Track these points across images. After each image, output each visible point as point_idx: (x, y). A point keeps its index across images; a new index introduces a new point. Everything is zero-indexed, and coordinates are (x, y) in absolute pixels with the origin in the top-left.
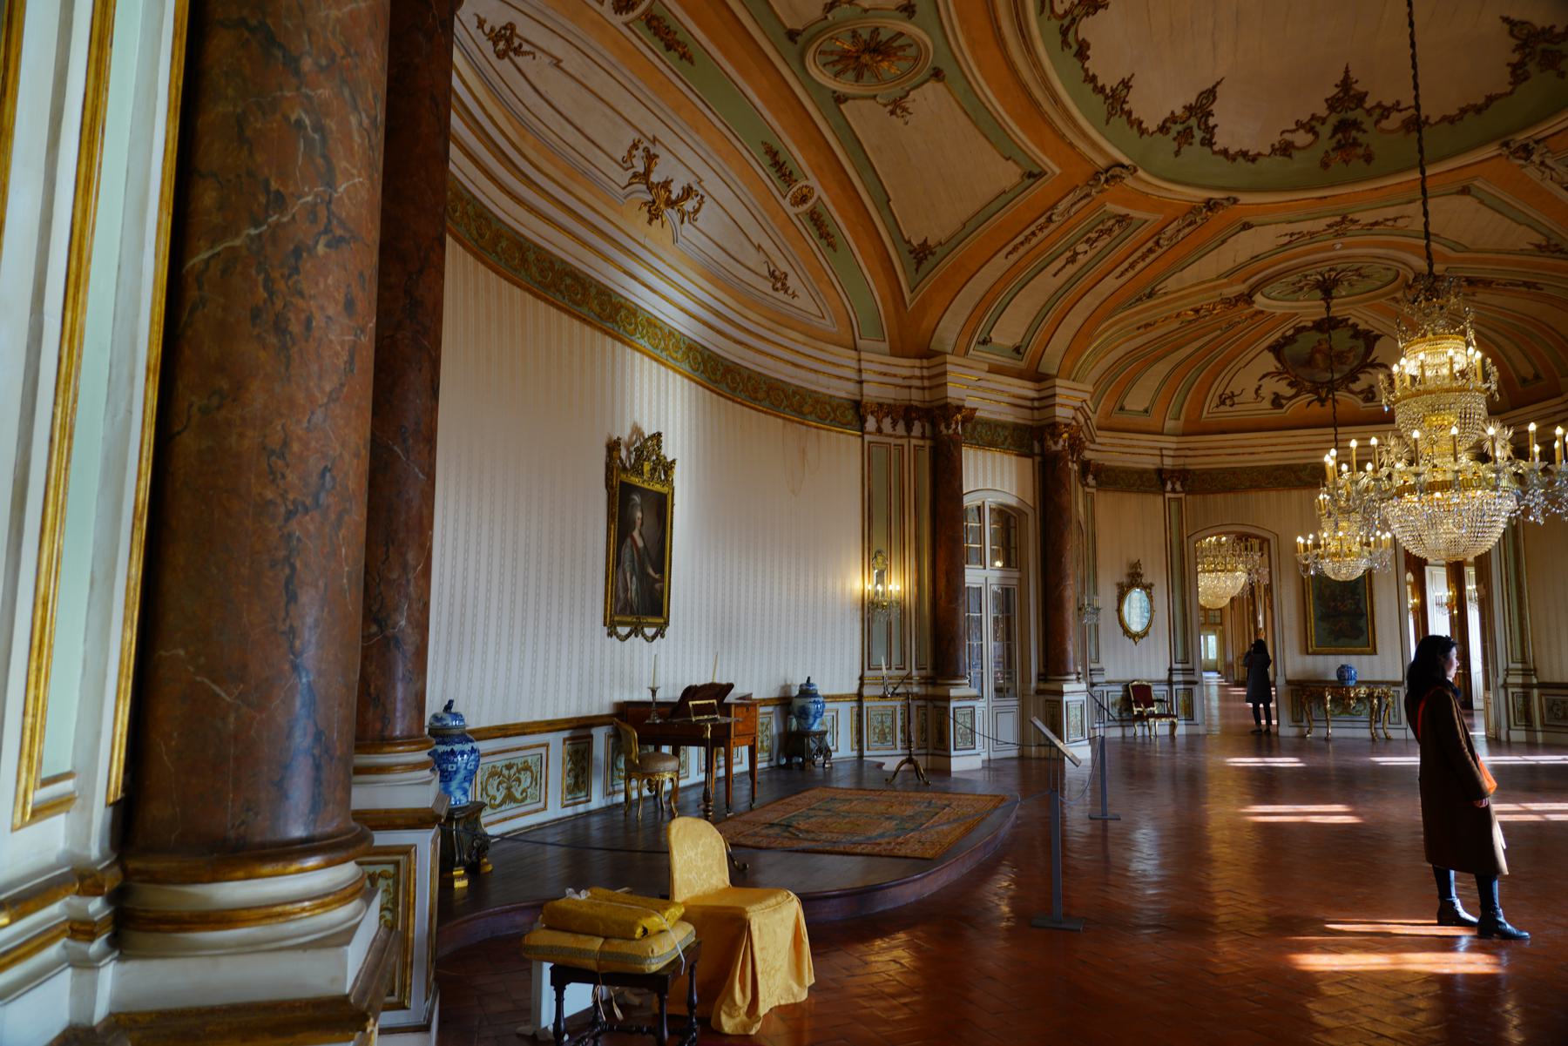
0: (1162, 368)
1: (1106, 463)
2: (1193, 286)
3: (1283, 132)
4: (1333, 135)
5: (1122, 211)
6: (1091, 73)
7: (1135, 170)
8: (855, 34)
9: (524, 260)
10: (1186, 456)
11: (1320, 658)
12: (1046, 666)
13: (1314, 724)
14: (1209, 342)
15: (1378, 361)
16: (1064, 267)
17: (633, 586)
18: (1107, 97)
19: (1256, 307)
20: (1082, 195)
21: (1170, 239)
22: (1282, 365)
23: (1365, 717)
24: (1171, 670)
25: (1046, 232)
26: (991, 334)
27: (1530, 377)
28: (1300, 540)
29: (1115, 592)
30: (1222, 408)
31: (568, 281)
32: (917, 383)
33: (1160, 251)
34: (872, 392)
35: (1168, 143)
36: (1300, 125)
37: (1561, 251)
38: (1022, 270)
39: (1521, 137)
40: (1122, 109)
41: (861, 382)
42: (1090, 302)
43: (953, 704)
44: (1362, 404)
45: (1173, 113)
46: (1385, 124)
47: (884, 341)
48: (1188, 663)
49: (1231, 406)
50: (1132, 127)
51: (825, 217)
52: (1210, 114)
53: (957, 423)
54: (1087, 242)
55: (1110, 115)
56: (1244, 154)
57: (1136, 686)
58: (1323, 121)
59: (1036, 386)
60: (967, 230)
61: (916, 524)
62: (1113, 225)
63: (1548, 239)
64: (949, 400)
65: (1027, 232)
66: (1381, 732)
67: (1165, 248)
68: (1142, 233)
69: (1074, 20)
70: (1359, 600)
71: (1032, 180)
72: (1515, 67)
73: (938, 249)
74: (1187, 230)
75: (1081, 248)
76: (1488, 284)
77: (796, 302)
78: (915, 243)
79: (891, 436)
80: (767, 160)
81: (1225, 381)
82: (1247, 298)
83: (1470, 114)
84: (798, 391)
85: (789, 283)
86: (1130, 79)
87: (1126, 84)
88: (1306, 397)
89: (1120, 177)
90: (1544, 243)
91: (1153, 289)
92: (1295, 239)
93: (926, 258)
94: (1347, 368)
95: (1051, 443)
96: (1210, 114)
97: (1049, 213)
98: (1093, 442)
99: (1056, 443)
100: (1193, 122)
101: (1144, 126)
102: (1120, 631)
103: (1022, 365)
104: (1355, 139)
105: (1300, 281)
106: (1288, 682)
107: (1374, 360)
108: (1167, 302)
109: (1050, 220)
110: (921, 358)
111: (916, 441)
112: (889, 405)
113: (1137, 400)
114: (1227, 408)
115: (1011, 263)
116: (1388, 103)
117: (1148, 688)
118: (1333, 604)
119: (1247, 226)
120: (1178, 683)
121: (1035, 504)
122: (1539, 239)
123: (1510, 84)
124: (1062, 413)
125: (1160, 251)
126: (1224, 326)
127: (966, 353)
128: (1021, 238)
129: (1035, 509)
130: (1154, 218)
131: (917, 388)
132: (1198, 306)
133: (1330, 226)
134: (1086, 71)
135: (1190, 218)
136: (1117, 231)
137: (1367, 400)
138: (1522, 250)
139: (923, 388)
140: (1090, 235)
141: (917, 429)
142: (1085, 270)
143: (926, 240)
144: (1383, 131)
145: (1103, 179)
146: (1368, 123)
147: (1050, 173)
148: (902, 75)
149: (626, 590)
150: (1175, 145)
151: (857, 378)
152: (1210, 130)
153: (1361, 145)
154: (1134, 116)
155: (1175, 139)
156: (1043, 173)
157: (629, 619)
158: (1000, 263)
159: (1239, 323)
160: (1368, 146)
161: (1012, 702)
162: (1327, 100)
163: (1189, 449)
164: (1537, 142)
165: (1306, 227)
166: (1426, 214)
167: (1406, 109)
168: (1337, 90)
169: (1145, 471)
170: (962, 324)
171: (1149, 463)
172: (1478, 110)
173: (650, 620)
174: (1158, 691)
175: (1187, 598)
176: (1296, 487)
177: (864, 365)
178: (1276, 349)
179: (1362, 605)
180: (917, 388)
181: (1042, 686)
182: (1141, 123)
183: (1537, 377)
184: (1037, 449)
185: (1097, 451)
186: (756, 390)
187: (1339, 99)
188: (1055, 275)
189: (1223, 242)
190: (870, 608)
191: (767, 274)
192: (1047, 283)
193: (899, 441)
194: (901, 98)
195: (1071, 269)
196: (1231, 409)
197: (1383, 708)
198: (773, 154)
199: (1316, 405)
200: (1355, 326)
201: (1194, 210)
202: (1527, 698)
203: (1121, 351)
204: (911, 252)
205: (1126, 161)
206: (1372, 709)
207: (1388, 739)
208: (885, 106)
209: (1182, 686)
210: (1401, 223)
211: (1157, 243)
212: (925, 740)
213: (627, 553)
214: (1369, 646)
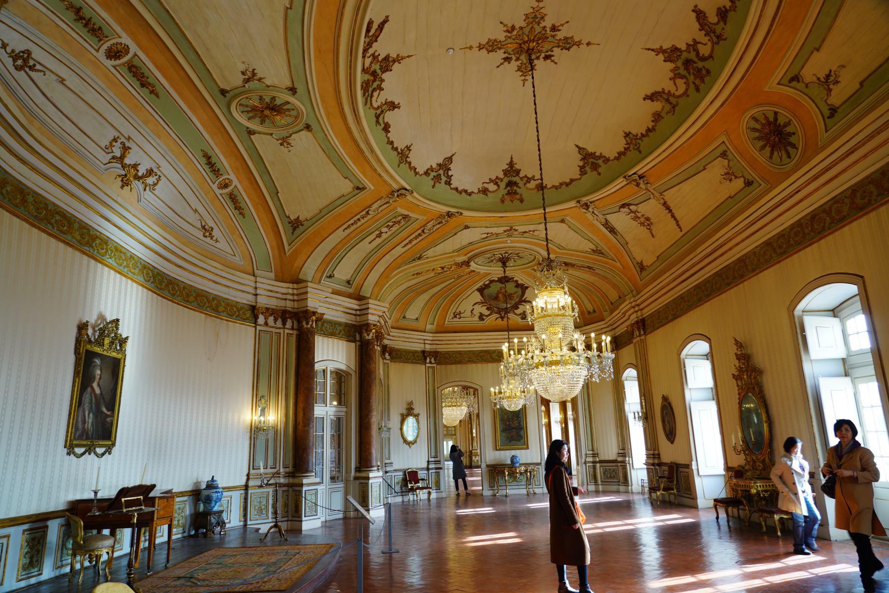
0: (425, 297)
1: (396, 347)
2: (441, 255)
3: (483, 183)
4: (506, 188)
5: (406, 213)
6: (391, 140)
7: (412, 193)
8: (261, 98)
9: (24, 201)
10: (437, 344)
11: (502, 452)
12: (360, 463)
13: (500, 488)
14: (449, 284)
15: (527, 299)
16: (375, 239)
17: (90, 419)
18: (399, 153)
19: (472, 268)
20: (385, 202)
21: (430, 230)
23: (524, 483)
24: (428, 462)
25: (366, 219)
26: (334, 273)
27: (591, 311)
28: (492, 390)
30: (455, 319)
31: (58, 218)
32: (290, 297)
33: (424, 235)
34: (263, 301)
35: (428, 181)
36: (491, 181)
37: (602, 253)
38: (352, 239)
39: (584, 199)
40: (406, 161)
41: (256, 295)
42: (388, 259)
43: (305, 488)
44: (521, 320)
45: (431, 166)
46: (528, 185)
47: (272, 272)
49: (460, 318)
50: (411, 170)
51: (239, 198)
52: (449, 169)
53: (313, 321)
54: (387, 227)
55: (400, 163)
56: (466, 191)
57: (410, 472)
58: (502, 180)
59: (358, 302)
60: (322, 214)
61: (287, 380)
62: (401, 220)
63: (597, 247)
64: (308, 308)
65: (356, 218)
66: (531, 490)
67: (427, 234)
68: (415, 226)
69: (382, 111)
71: (359, 191)
73: (305, 223)
74: (438, 226)
75: (384, 230)
76: (573, 265)
77: (217, 245)
78: (292, 218)
79: (273, 327)
80: (203, 161)
82: (467, 263)
83: (564, 186)
84: (216, 298)
85: (214, 234)
86: (410, 146)
87: (408, 148)
88: (495, 316)
89: (405, 195)
90: (595, 249)
91: (421, 255)
92: (489, 236)
93: (298, 227)
94: (513, 302)
95: (365, 335)
96: (449, 169)
97: (367, 210)
98: (389, 335)
99: (368, 335)
100: (441, 172)
101: (417, 170)
102: (402, 440)
103: (351, 291)
104: (515, 190)
105: (492, 257)
106: (488, 466)
107: (525, 299)
108: (428, 262)
109: (368, 213)
110: (293, 283)
111: (288, 330)
112: (273, 309)
113: (413, 313)
115: (346, 234)
116: (530, 176)
117: (416, 472)
118: (508, 423)
119: (467, 227)
120: (432, 469)
121: (356, 369)
122: (593, 247)
123: (580, 175)
124: (372, 319)
125: (424, 235)
126: (456, 277)
127: (320, 282)
128: (352, 221)
129: (356, 372)
130: (422, 218)
131: (290, 300)
132: (443, 265)
133: (505, 231)
134: (388, 138)
135: (440, 220)
136: (403, 223)
139: (294, 301)
140: (389, 223)
141: (289, 324)
142: (386, 242)
143: (298, 217)
144: (527, 188)
145: (396, 195)
146: (521, 184)
147: (368, 188)
148: (288, 125)
149: (84, 422)
150: (432, 183)
151: (254, 292)
152: (449, 177)
153: (518, 194)
155: (432, 179)
156: (364, 188)
157: (85, 443)
158: (340, 234)
159: (463, 276)
160: (521, 195)
161: (341, 485)
162: (503, 170)
164: (591, 203)
165: (494, 230)
166: (546, 229)
167: (537, 180)
169: (416, 352)
170: (318, 265)
171: (418, 347)
172: (567, 185)
173: (101, 443)
174: (422, 474)
175: (437, 421)
176: (491, 362)
177: (258, 285)
178: (481, 290)
179: (522, 424)
180: (290, 300)
181: (358, 475)
182: (416, 169)
183: (594, 311)
184: (358, 338)
185: (391, 340)
186: (188, 295)
187: (508, 171)
188: (370, 243)
189: (456, 234)
190: (255, 431)
191: (200, 227)
192: (365, 247)
193: (278, 331)
194: (287, 137)
195: (378, 240)
198: (208, 158)
199: (500, 319)
200: (517, 281)
201: (441, 216)
202: (594, 468)
203: (404, 287)
204: (289, 223)
205: (408, 188)
206: (527, 478)
207: (535, 493)
208: (278, 140)
209: (434, 471)
210: (536, 233)
211: (423, 231)
212: (287, 512)
213: (87, 397)
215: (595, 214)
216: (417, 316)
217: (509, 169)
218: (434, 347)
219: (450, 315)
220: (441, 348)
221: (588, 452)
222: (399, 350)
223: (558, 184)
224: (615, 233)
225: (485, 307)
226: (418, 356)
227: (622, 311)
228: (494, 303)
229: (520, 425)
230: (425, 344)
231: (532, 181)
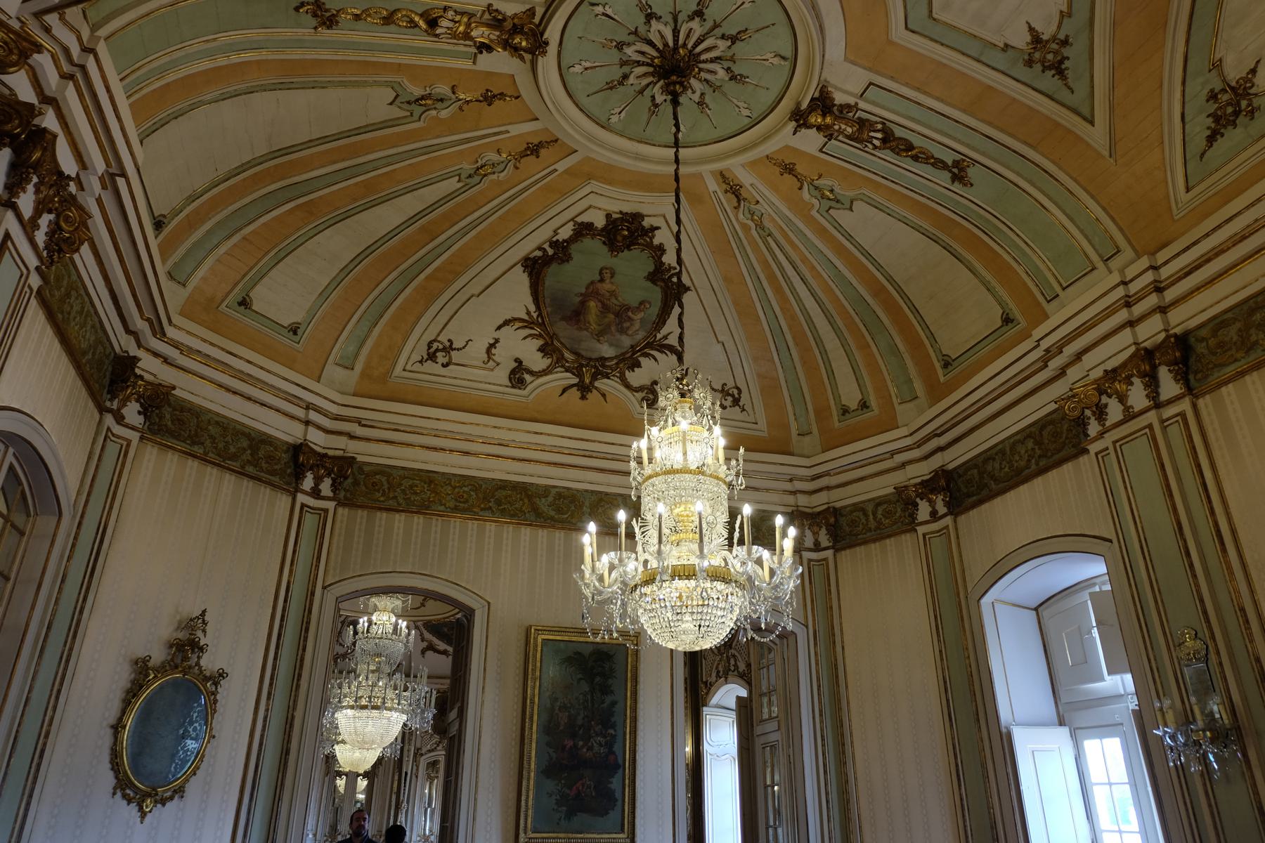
22: (538, 308)
27: (853, 405)
29: (124, 677)
49: (444, 366)
70: (614, 737)
81: (442, 318)
88: (563, 378)
94: (627, 342)
98: (159, 332)
107: (665, 337)
114: (437, 368)
118: (569, 743)
126: (468, 167)
163: (359, 422)
169: (266, 440)
175: (298, 714)
178: (535, 267)
179: (617, 748)
183: (864, 405)
196: (443, 371)
199: (575, 393)
214: (622, 831)
216: (297, 317)
218: (341, 442)
219: (414, 348)
222: (196, 412)
225: (539, 343)
226: (270, 458)
227: (1045, 344)
228: (564, 331)
229: (611, 752)
230: (307, 423)
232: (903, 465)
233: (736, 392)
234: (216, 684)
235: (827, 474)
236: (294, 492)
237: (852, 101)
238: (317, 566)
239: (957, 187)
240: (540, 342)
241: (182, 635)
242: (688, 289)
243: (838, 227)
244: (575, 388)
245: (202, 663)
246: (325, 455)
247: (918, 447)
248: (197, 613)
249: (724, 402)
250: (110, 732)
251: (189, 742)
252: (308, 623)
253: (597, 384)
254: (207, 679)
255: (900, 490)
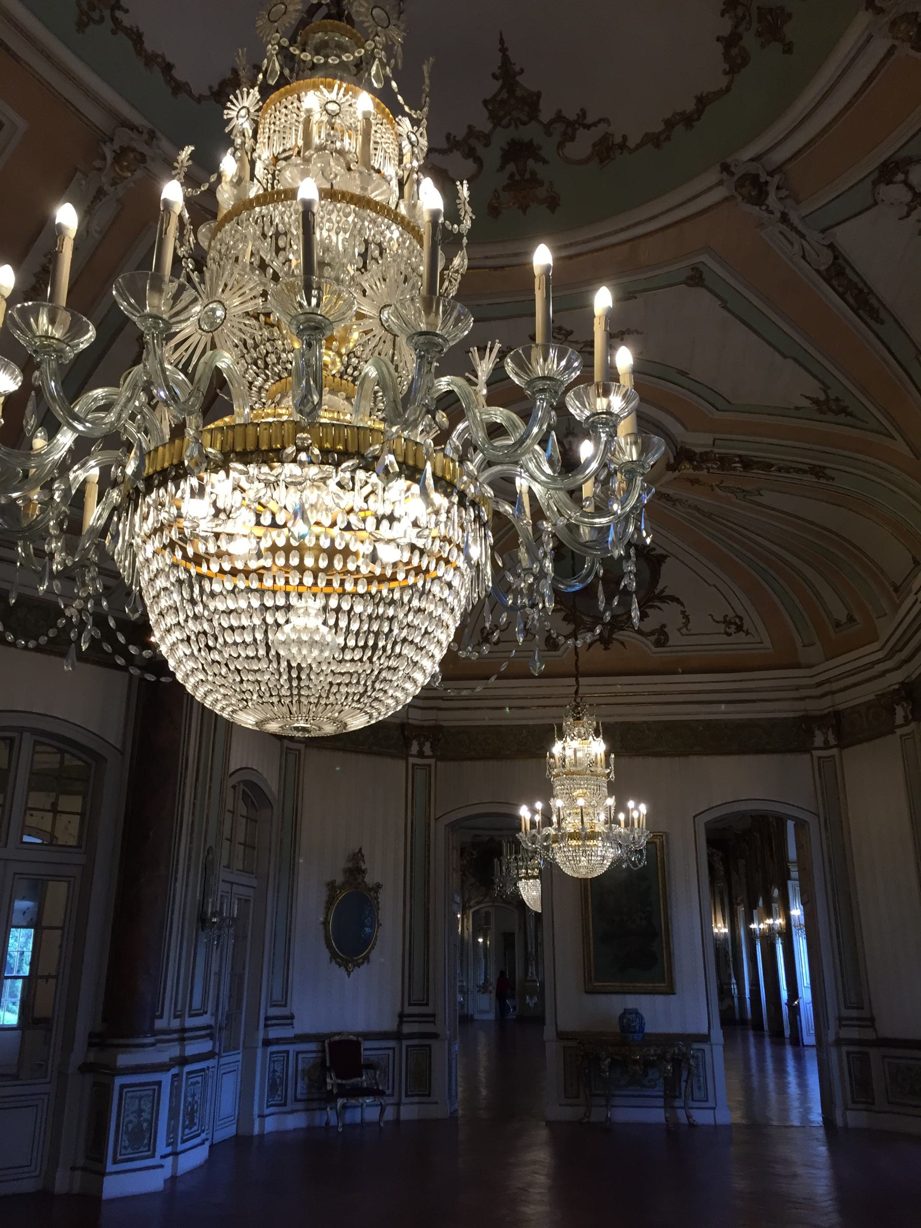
4: (502, 168)
7: (152, 135)
11: (602, 998)
15: (667, 592)
24: (401, 1016)
27: (843, 619)
28: (524, 812)
48: (427, 1004)
57: (340, 1042)
58: (486, 140)
63: (826, 388)
66: (681, 1115)
72: (730, 42)
90: (822, 397)
104: (533, 173)
107: (663, 591)
116: (571, 116)
117: (357, 1044)
120: (411, 1036)
123: (726, 73)
137: (659, 644)
138: (797, 408)
153: (541, 184)
154: (149, 46)
162: (486, 103)
167: (595, 124)
168: (498, 84)
172: (688, 120)
174: (369, 1050)
183: (851, 619)
197: (684, 1077)
207: (692, 1125)
215: (794, 229)
217: (504, 95)
218: (432, 715)
220: (448, 719)
221: (846, 1013)
223: (661, 127)
224: (874, 314)
231: (581, 132)
232: (883, 674)
233: (737, 620)
234: (377, 892)
235: (828, 681)
236: (406, 757)
237: (708, 450)
238: (429, 806)
239: (823, 481)
240: (563, 614)
241: (350, 865)
242: (665, 557)
243: (760, 505)
244: (598, 643)
245: (366, 880)
246: (422, 727)
247: (890, 659)
248: (357, 850)
249: (728, 630)
250: (321, 927)
251: (367, 929)
252: (429, 845)
253: (614, 636)
254: (370, 890)
255: (880, 697)
